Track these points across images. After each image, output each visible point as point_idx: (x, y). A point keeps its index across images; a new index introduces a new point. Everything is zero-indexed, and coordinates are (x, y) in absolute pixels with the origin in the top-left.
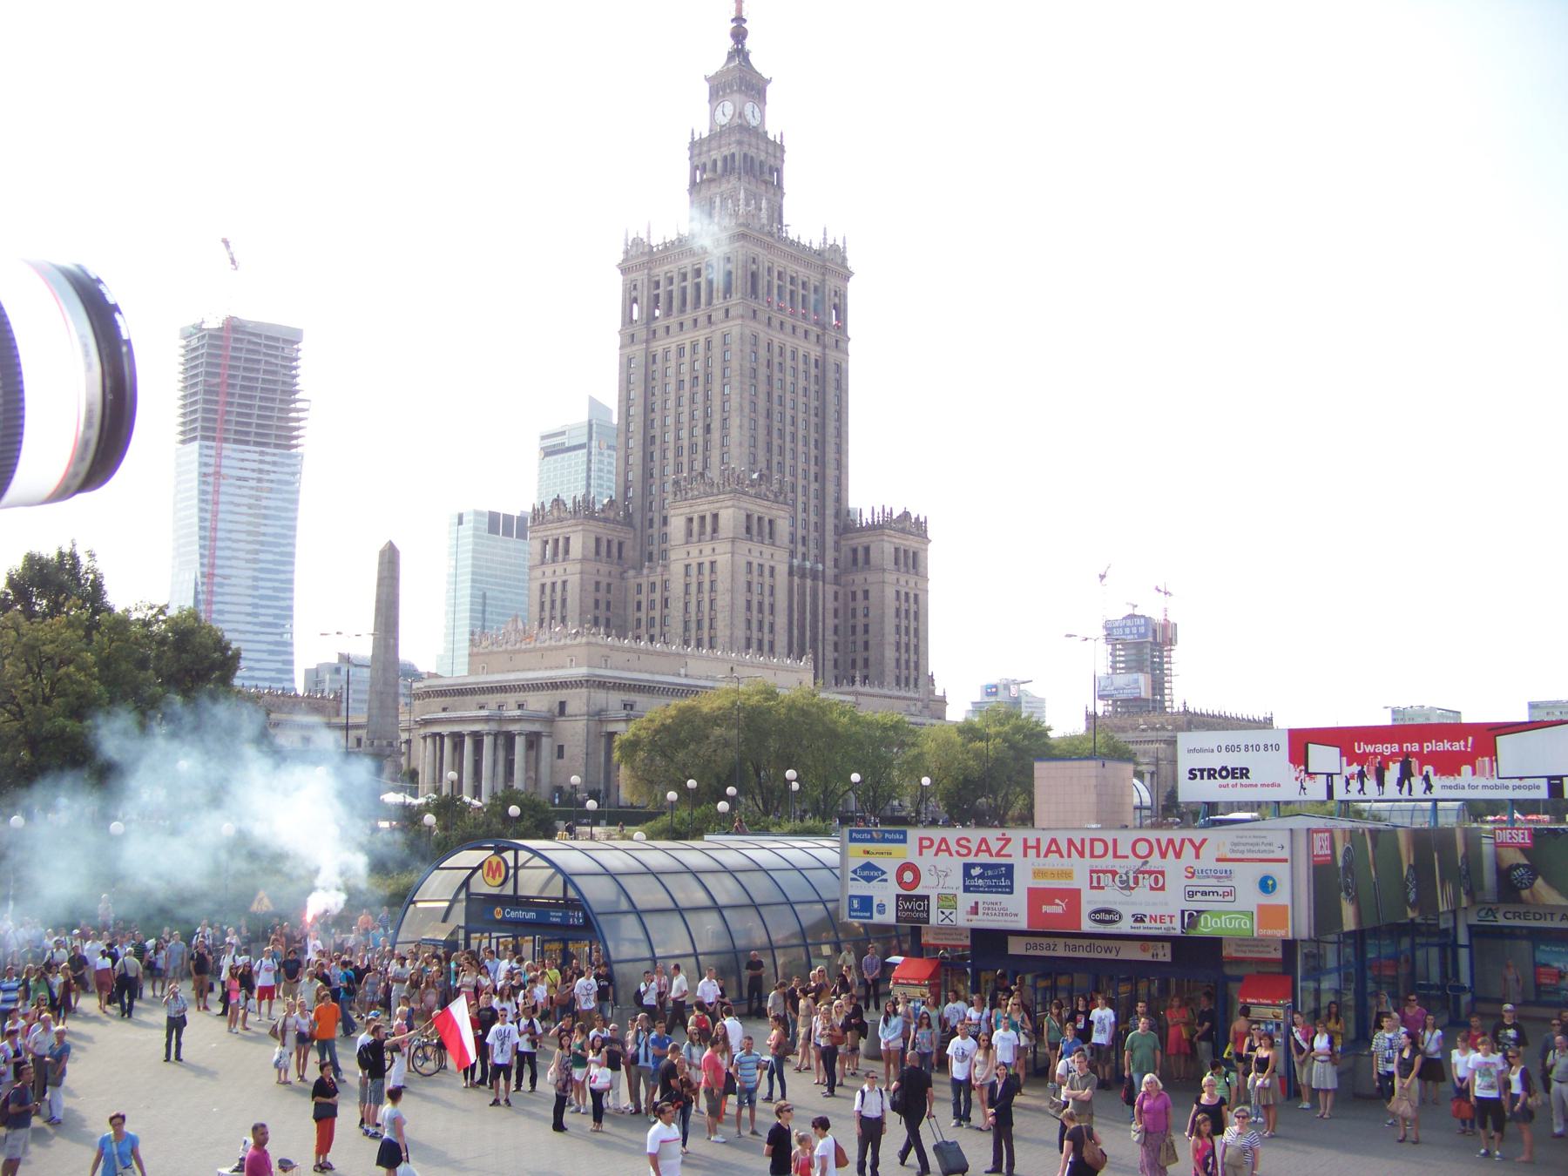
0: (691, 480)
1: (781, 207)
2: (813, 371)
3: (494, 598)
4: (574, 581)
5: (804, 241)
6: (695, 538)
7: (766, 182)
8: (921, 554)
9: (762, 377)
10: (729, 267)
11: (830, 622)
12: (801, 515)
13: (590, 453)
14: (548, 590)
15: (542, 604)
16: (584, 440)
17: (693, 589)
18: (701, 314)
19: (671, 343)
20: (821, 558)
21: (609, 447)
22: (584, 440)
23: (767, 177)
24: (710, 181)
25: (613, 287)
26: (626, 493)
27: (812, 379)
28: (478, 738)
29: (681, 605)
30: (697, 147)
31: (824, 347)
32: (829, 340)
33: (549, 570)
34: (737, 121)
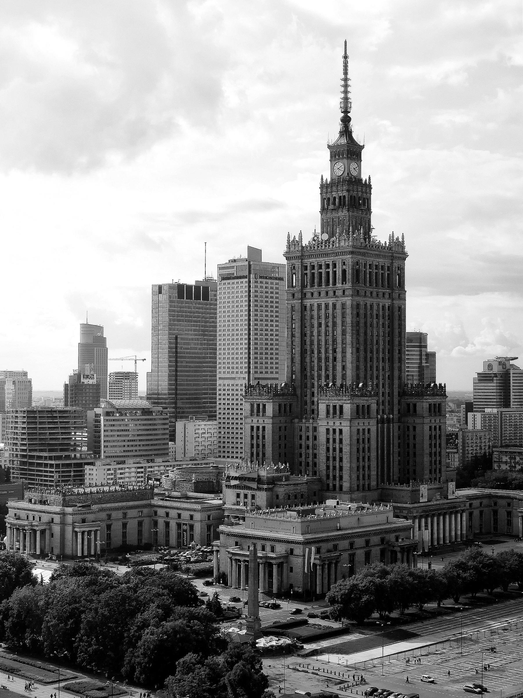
3: (182, 339)
5: (383, 242)
9: (362, 325)
10: (344, 267)
11: (396, 442)
13: (250, 282)
17: (331, 441)
19: (315, 302)
20: (391, 411)
21: (261, 277)
26: (292, 377)
30: (325, 187)
32: (395, 295)
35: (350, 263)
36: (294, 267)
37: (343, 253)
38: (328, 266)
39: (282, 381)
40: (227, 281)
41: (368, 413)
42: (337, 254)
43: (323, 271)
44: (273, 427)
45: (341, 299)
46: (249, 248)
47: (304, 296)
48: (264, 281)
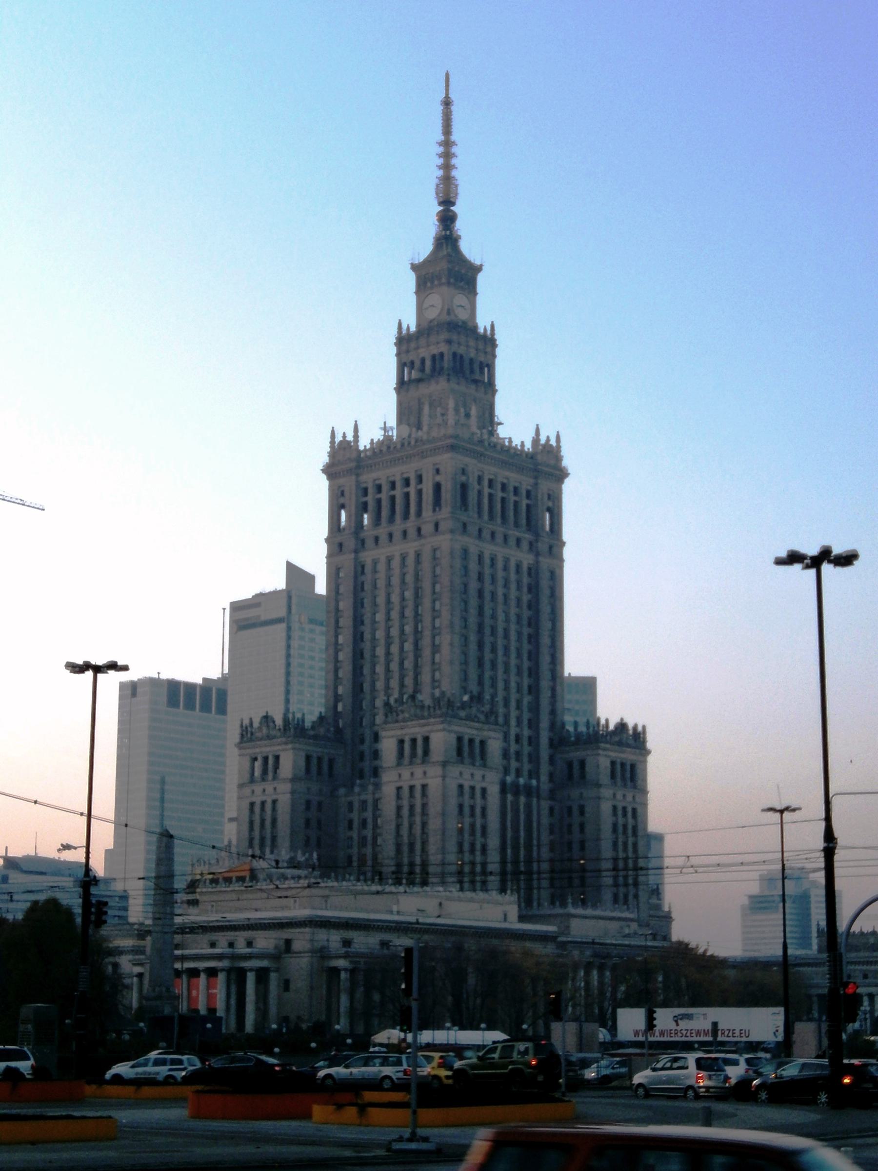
0: (399, 701)
4: (285, 800)
5: (516, 442)
6: (406, 759)
7: (475, 382)
8: (639, 767)
10: (438, 478)
11: (545, 838)
12: (513, 731)
14: (257, 809)
15: (251, 823)
17: (405, 812)
18: (411, 525)
20: (534, 773)
21: (312, 621)
22: (283, 613)
23: (477, 376)
24: (419, 381)
25: (320, 489)
26: (336, 707)
27: (525, 589)
28: (212, 973)
31: (538, 554)
32: (542, 546)
33: (258, 788)
34: (445, 318)
36: (342, 494)
37: (436, 451)
38: (407, 482)
42: (423, 455)
43: (398, 493)
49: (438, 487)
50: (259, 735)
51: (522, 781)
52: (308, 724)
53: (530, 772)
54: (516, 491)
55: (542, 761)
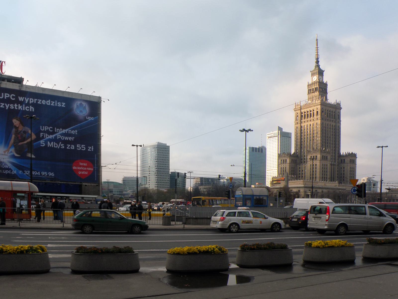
1: (327, 96)
2: (334, 128)
5: (332, 103)
10: (317, 110)
13: (278, 138)
14: (282, 168)
16: (278, 135)
19: (306, 124)
20: (335, 162)
21: (283, 136)
23: (324, 91)
24: (312, 92)
29: (310, 171)
31: (336, 123)
33: (282, 165)
35: (320, 108)
36: (298, 114)
38: (311, 111)
39: (293, 151)
40: (270, 139)
41: (327, 159)
42: (314, 106)
43: (309, 113)
44: (289, 167)
45: (316, 121)
46: (278, 127)
47: (301, 122)
48: (284, 137)
49: (317, 112)
50: (282, 156)
51: (333, 163)
52: (292, 154)
53: (334, 161)
54: (332, 112)
55: (336, 159)
